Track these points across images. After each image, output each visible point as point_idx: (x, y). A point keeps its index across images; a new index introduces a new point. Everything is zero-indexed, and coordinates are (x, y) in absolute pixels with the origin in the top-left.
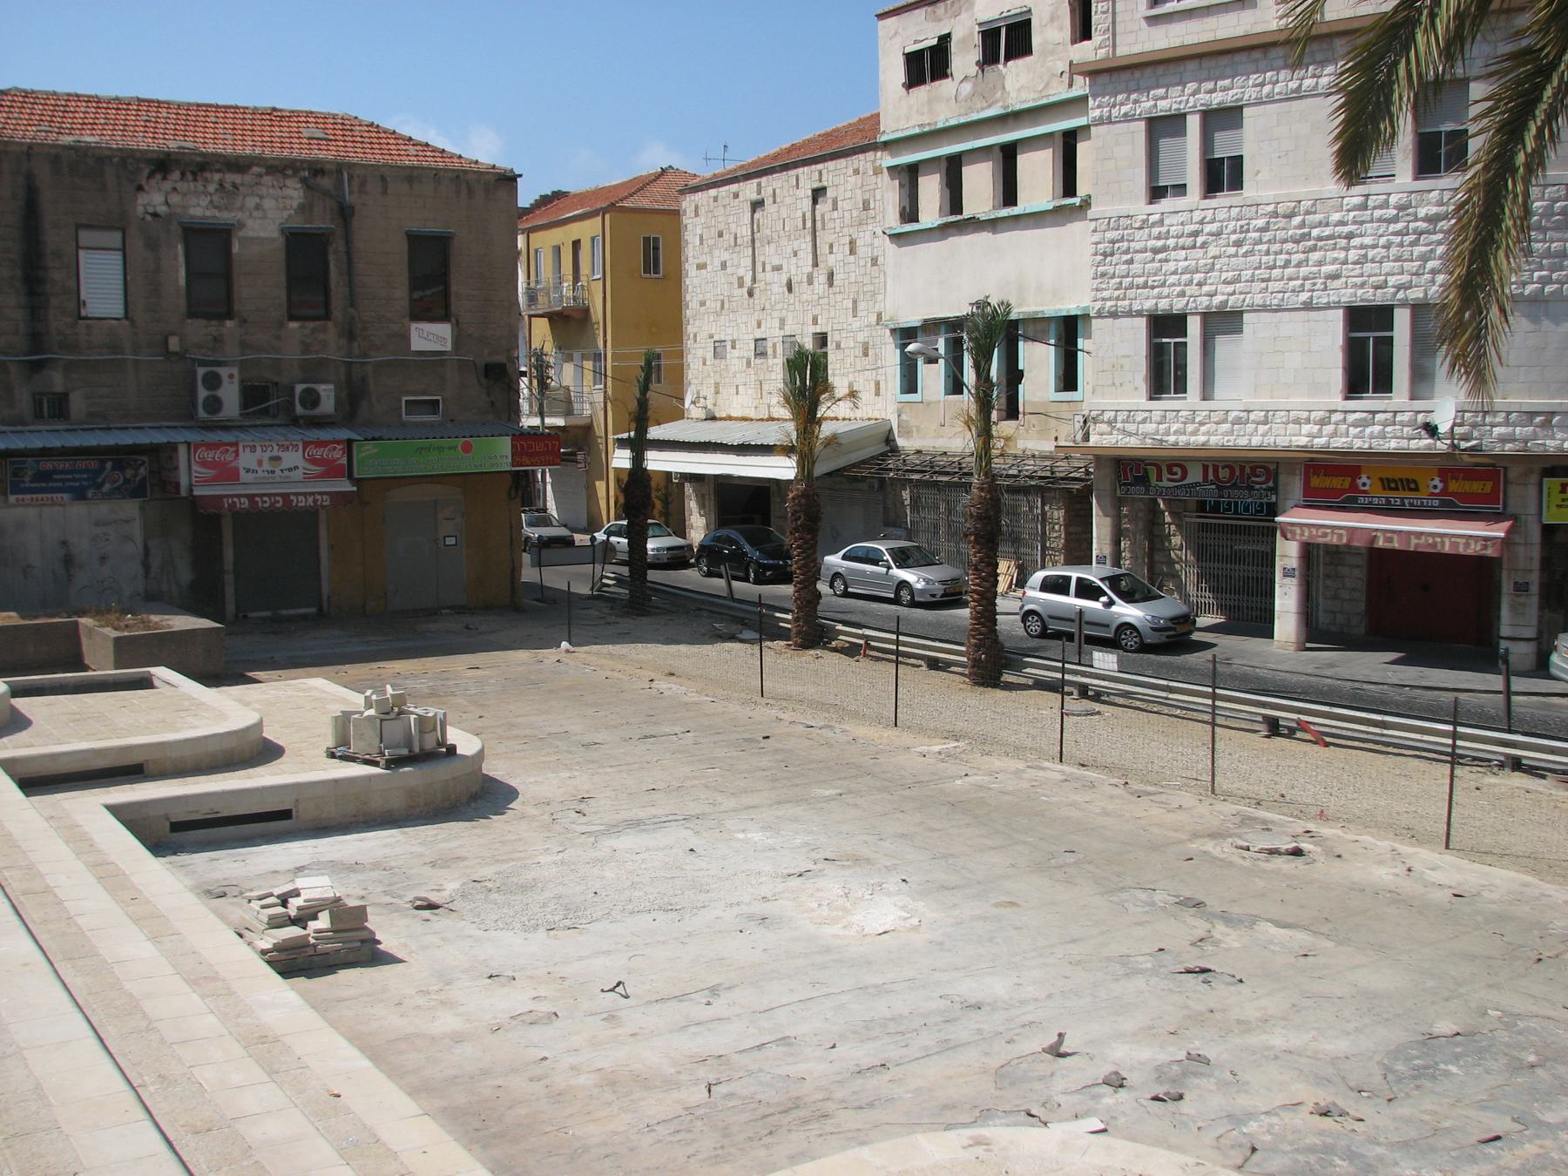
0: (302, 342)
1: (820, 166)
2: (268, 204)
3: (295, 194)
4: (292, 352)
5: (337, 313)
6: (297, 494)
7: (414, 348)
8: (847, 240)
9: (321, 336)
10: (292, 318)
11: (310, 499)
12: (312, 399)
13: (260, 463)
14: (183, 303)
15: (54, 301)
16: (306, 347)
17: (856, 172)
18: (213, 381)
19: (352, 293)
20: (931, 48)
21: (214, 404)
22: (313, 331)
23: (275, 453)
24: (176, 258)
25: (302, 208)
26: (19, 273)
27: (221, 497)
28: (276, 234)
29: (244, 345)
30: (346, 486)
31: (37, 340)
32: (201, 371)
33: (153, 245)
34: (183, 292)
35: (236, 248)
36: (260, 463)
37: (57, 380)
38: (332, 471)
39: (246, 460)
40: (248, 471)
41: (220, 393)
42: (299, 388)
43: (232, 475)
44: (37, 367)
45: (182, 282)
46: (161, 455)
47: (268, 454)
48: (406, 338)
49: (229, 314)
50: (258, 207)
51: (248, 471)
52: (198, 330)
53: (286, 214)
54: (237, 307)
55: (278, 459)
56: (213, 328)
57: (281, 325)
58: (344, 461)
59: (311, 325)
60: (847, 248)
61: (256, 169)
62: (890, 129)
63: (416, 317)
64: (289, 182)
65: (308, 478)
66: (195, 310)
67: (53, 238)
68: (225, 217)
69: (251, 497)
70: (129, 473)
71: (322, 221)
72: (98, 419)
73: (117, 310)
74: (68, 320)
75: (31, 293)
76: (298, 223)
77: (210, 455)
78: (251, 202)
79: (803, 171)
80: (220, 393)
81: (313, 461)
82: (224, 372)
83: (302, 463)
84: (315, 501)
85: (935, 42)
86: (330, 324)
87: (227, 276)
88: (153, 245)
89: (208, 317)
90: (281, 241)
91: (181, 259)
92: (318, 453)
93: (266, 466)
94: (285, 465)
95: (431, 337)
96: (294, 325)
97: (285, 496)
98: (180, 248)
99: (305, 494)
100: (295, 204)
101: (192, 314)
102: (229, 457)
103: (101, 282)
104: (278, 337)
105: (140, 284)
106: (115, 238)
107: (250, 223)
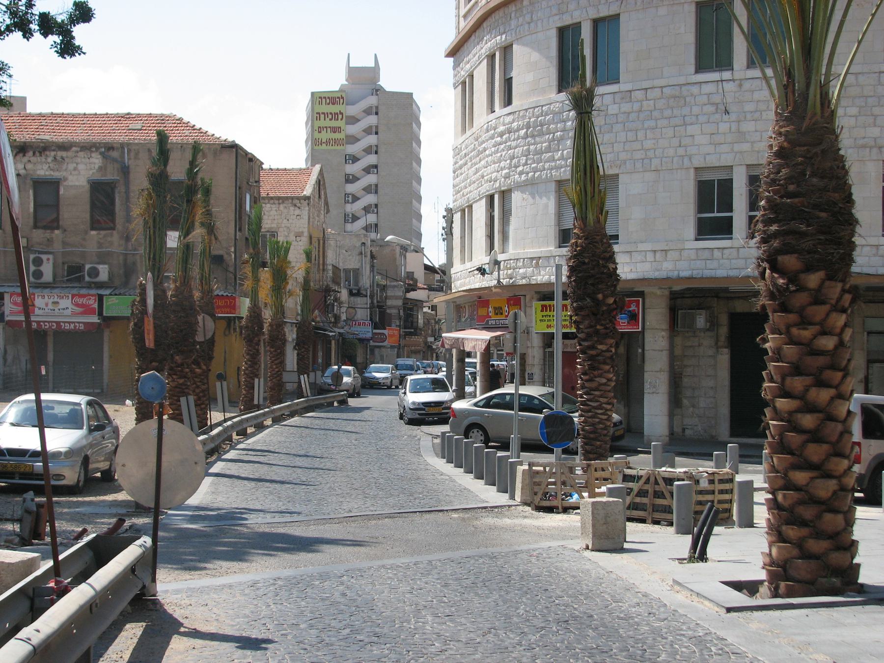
0: (99, 242)
2: (81, 167)
3: (97, 161)
4: (92, 247)
5: (119, 227)
6: (65, 322)
9: (109, 239)
10: (93, 229)
11: (72, 326)
12: (94, 272)
13: (47, 305)
16: (100, 245)
18: (38, 262)
21: (38, 274)
22: (105, 236)
23: (56, 300)
24: (29, 198)
25: (100, 168)
28: (85, 183)
29: (65, 244)
30: (95, 319)
34: (32, 216)
35: (62, 192)
36: (47, 305)
38: (88, 311)
40: (40, 309)
41: (42, 268)
42: (87, 267)
45: (32, 210)
47: (52, 300)
49: (58, 228)
50: (75, 169)
51: (40, 309)
52: (39, 235)
53: (91, 172)
54: (61, 223)
55: (58, 303)
56: (48, 234)
57: (86, 233)
58: (96, 306)
59: (103, 232)
64: (93, 155)
65: (74, 314)
68: (56, 175)
71: (112, 175)
76: (98, 177)
78: (71, 166)
80: (42, 268)
81: (77, 305)
83: (70, 306)
84: (75, 326)
86: (115, 232)
87: (56, 206)
89: (45, 228)
91: (32, 197)
92: (80, 301)
93: (50, 306)
94: (61, 306)
96: (94, 233)
97: (58, 323)
98: (31, 192)
99: (69, 323)
100: (97, 167)
101: (36, 226)
104: (84, 239)
107: (70, 178)
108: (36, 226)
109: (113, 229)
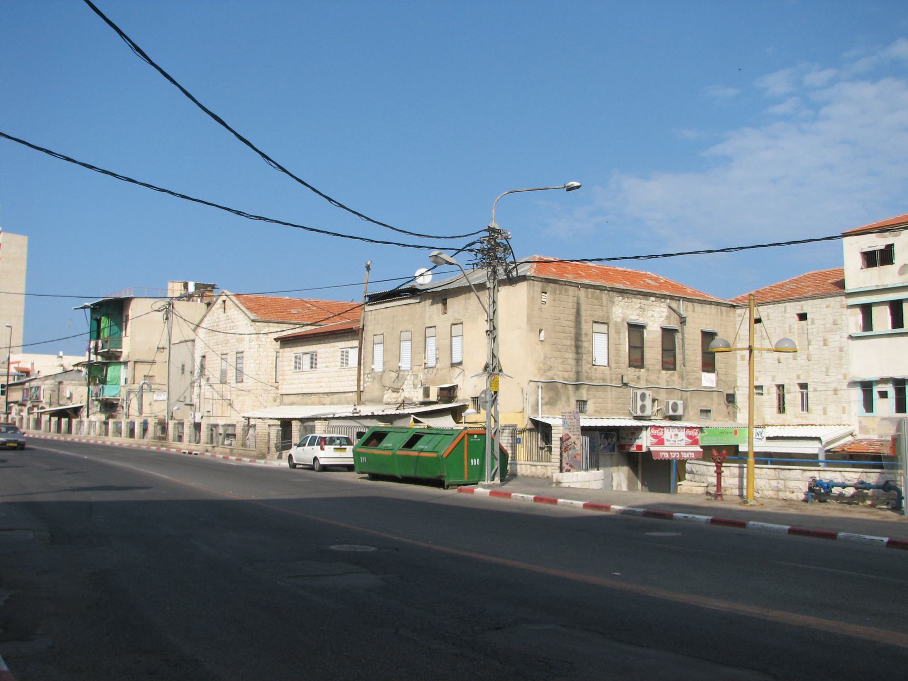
1: (802, 303)
2: (656, 314)
5: (678, 367)
7: (704, 385)
8: (822, 339)
10: (664, 369)
15: (585, 357)
16: (668, 382)
17: (828, 307)
18: (643, 396)
19: (684, 359)
20: (881, 251)
21: (643, 408)
22: (671, 375)
25: (667, 317)
26: (573, 343)
27: (659, 452)
29: (647, 381)
33: (618, 332)
35: (645, 336)
37: (584, 394)
39: (667, 435)
43: (661, 442)
44: (577, 387)
48: (700, 379)
57: (660, 372)
59: (670, 372)
60: (822, 343)
61: (652, 299)
62: (850, 287)
63: (703, 371)
67: (585, 327)
69: (669, 452)
70: (610, 440)
71: (674, 325)
72: (598, 413)
74: (589, 366)
75: (577, 353)
78: (650, 313)
79: (790, 305)
81: (689, 437)
85: (883, 247)
88: (618, 332)
89: (636, 367)
93: (673, 439)
95: (708, 380)
96: (664, 372)
102: (661, 433)
103: (599, 348)
104: (658, 378)
106: (603, 328)
108: (630, 366)
109: (674, 369)
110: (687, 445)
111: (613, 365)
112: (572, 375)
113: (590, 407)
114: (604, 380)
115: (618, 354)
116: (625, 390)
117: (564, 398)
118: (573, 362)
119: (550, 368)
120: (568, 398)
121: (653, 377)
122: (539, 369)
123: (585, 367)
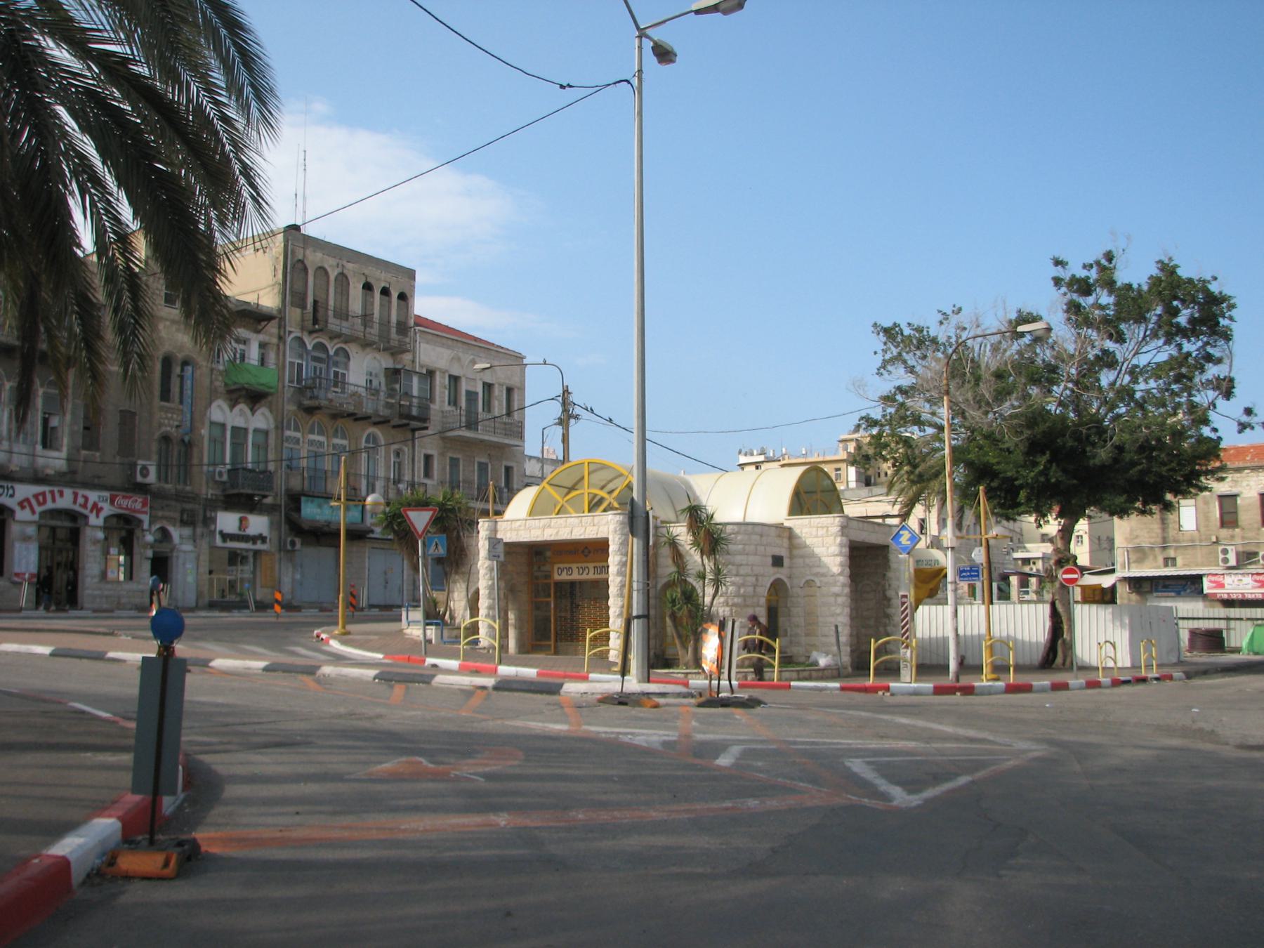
2: (1252, 483)
14: (1218, 523)
18: (1225, 552)
21: (1226, 560)
29: (1243, 538)
31: (1164, 540)
32: (1220, 548)
37: (1171, 553)
43: (1221, 586)
44: (1164, 548)
46: (1198, 579)
52: (1224, 533)
65: (1254, 588)
66: (1223, 524)
68: (1234, 491)
73: (1194, 528)
77: (1213, 578)
78: (1244, 484)
82: (1229, 548)
87: (1236, 513)
90: (1257, 498)
105: (1202, 517)
110: (1254, 588)
111: (1202, 529)
112: (1159, 540)
113: (1179, 561)
114: (1193, 541)
115: (1207, 519)
116: (1215, 546)
117: (1151, 557)
118: (1159, 531)
119: (1137, 537)
120: (1155, 557)
121: (1249, 534)
122: (1126, 539)
123: (1172, 533)
